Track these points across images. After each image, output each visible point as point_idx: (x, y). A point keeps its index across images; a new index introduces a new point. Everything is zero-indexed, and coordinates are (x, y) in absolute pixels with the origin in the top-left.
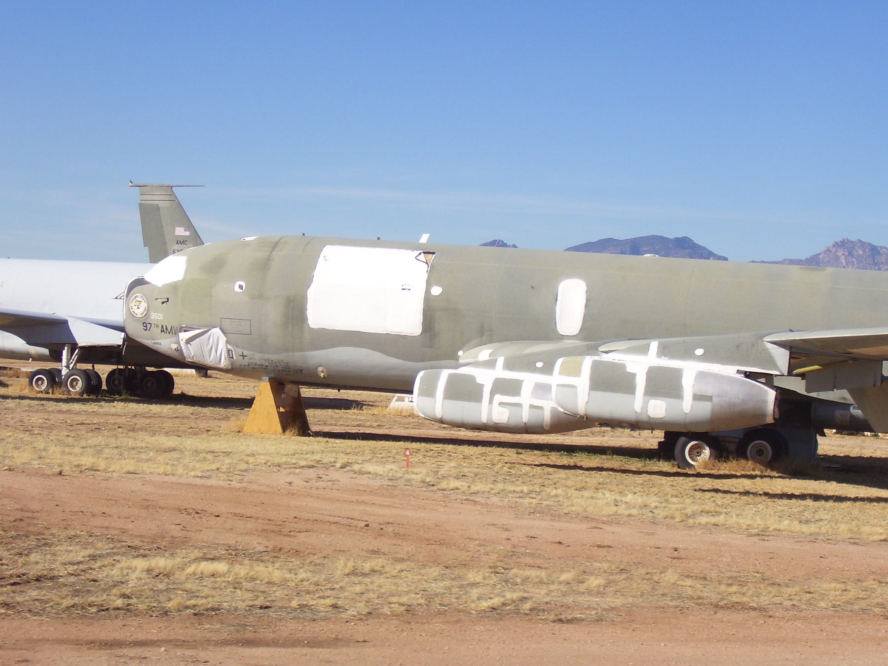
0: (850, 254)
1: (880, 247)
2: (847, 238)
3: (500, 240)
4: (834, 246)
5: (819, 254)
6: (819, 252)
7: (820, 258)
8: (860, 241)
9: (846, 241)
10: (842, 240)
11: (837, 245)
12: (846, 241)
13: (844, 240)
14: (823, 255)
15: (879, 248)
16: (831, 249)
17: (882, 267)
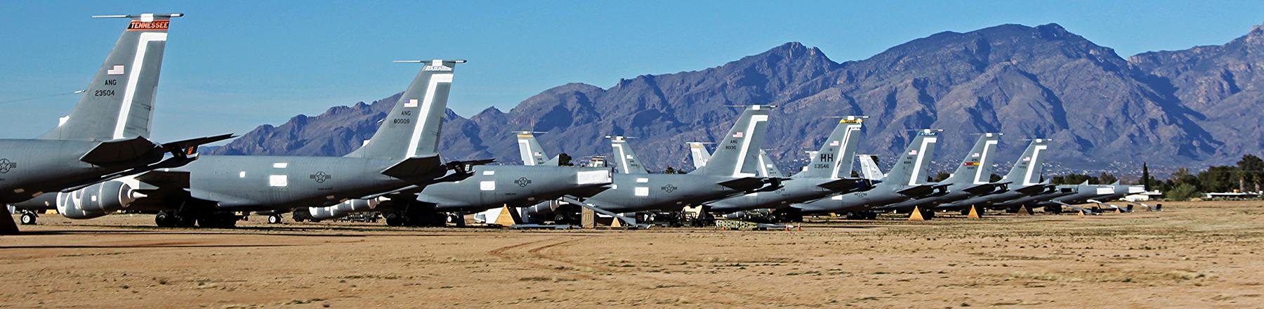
3: (796, 43)
5: (1245, 37)
6: (1245, 34)
7: (1246, 43)
14: (1250, 38)
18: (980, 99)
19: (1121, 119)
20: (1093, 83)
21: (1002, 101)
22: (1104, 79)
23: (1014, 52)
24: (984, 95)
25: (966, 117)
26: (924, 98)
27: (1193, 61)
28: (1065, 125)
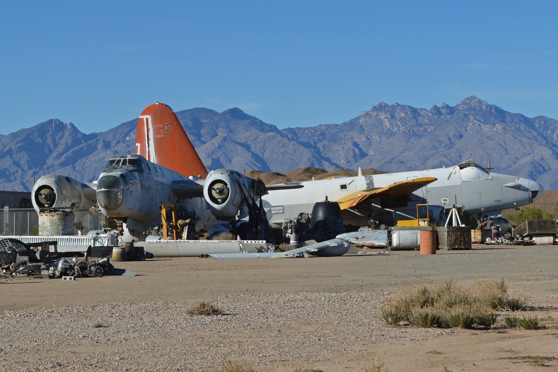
0: (392, 117)
1: (420, 109)
2: (383, 102)
3: (56, 119)
4: (373, 110)
5: (359, 118)
7: (360, 122)
8: (399, 105)
9: (383, 104)
10: (379, 104)
12: (383, 104)
13: (381, 104)
14: (363, 119)
15: (419, 110)
16: (370, 113)
17: (428, 128)
20: (283, 149)
21: (227, 161)
23: (217, 127)
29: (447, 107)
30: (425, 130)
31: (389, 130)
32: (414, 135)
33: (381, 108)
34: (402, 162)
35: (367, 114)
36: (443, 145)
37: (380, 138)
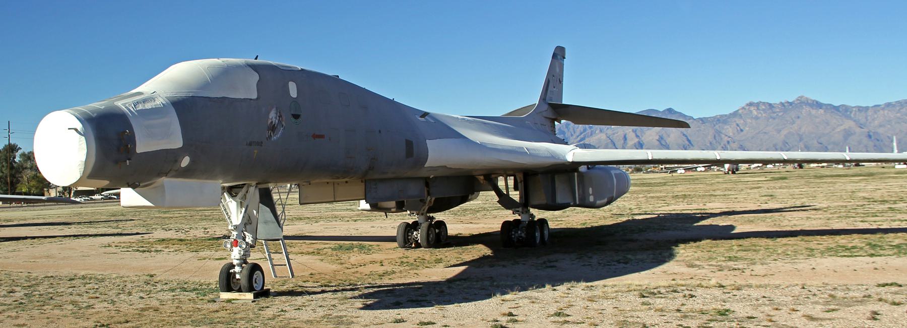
1: (775, 104)
5: (738, 110)
6: (737, 109)
11: (747, 105)
16: (745, 107)
18: (660, 136)
19: (714, 142)
20: (698, 129)
22: (703, 127)
24: (660, 134)
25: (657, 143)
26: (637, 136)
27: (718, 120)
28: (692, 145)
29: (788, 102)
30: (777, 115)
31: (756, 116)
32: (771, 118)
33: (751, 104)
34: (765, 133)
35: (743, 108)
36: (789, 122)
37: (751, 120)
